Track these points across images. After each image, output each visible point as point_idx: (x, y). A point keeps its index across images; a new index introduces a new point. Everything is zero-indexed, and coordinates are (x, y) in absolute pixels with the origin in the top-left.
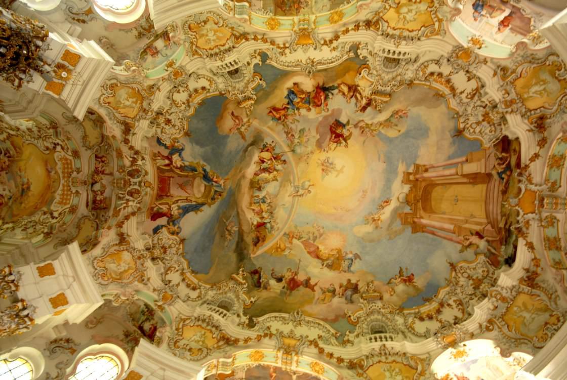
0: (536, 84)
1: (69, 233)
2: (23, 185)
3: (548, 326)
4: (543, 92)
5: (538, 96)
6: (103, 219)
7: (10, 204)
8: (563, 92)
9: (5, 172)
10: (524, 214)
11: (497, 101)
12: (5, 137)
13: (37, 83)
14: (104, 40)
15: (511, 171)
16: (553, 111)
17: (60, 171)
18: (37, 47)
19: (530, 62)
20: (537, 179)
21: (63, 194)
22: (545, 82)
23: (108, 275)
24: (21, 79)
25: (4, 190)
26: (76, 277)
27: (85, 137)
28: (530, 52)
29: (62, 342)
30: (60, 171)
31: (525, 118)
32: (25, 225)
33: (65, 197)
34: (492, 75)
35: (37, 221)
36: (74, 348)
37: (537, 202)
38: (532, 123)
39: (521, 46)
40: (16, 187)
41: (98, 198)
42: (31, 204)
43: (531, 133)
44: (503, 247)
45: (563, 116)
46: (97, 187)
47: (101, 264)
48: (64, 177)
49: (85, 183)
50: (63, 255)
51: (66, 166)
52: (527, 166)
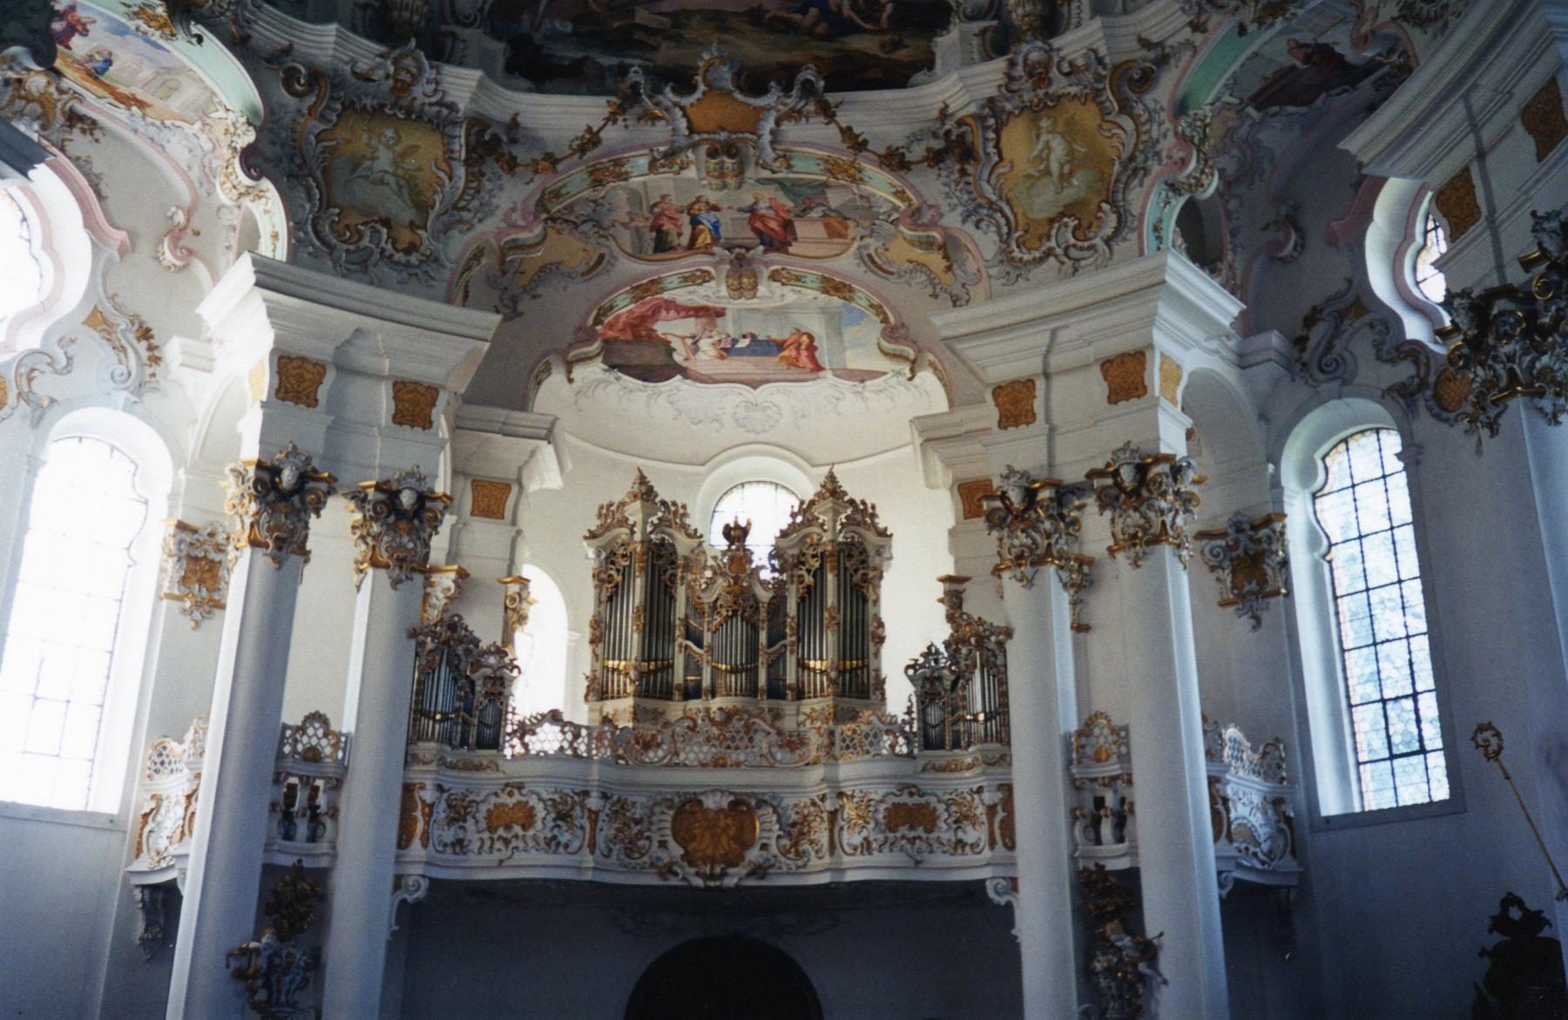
0: (1071, 152)
3: (385, 231)
4: (1042, 167)
5: (1036, 153)
8: (1020, 223)
10: (683, 109)
11: (1057, 42)
15: (828, 38)
16: (984, 184)
19: (1132, 158)
20: (791, 130)
22: (1065, 178)
28: (1156, 169)
31: (983, 107)
34: (1144, 35)
37: (723, 136)
38: (960, 123)
39: (1181, 154)
43: (936, 114)
44: (569, 28)
45: (960, 209)
52: (828, 112)
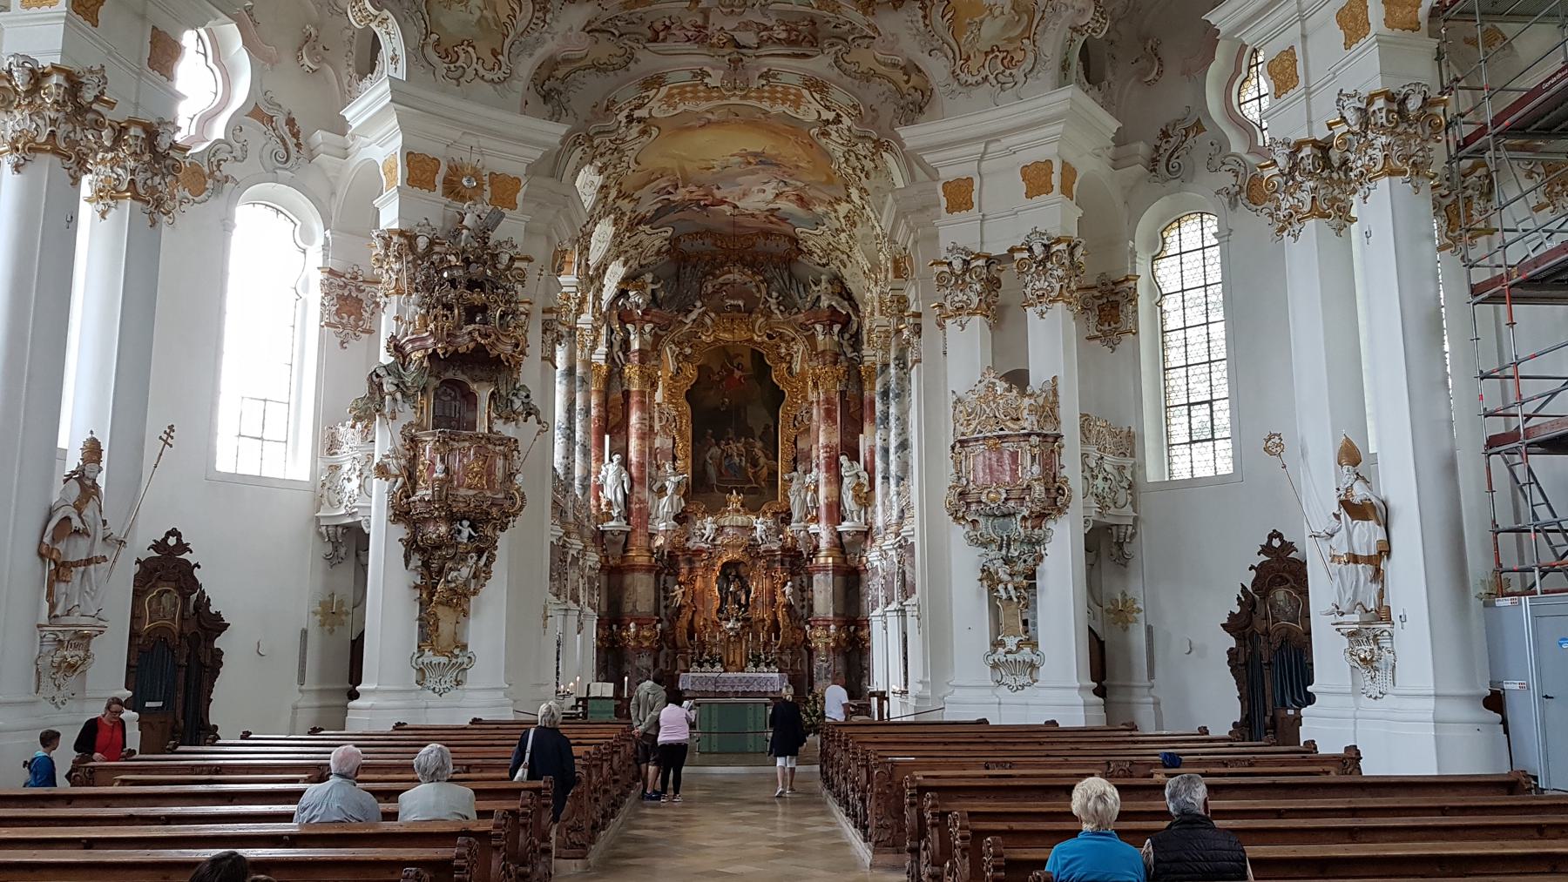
1: (883, 98)
2: (750, 163)
6: (848, 26)
7: (799, 184)
9: (715, 191)
12: (627, 200)
13: (511, 229)
14: (306, 60)
17: (704, 106)
18: (432, 243)
21: (773, 99)
23: (1010, 48)
24: (512, 259)
25: (764, 191)
26: (991, 138)
27: (599, 68)
29: (1165, 146)
30: (704, 106)
32: (854, 169)
33: (779, 95)
35: (846, 149)
36: (1187, 125)
40: (753, 173)
41: (783, 35)
42: (800, 151)
46: (742, 37)
47: (974, 64)
48: (723, 97)
49: (735, 64)
50: (927, 158)
51: (689, 95)
